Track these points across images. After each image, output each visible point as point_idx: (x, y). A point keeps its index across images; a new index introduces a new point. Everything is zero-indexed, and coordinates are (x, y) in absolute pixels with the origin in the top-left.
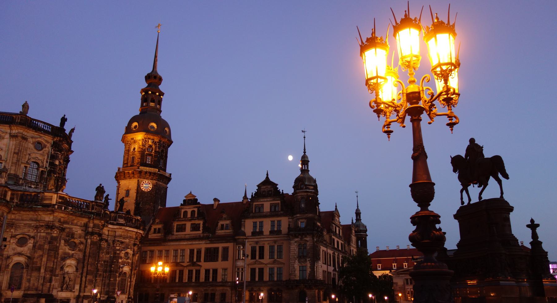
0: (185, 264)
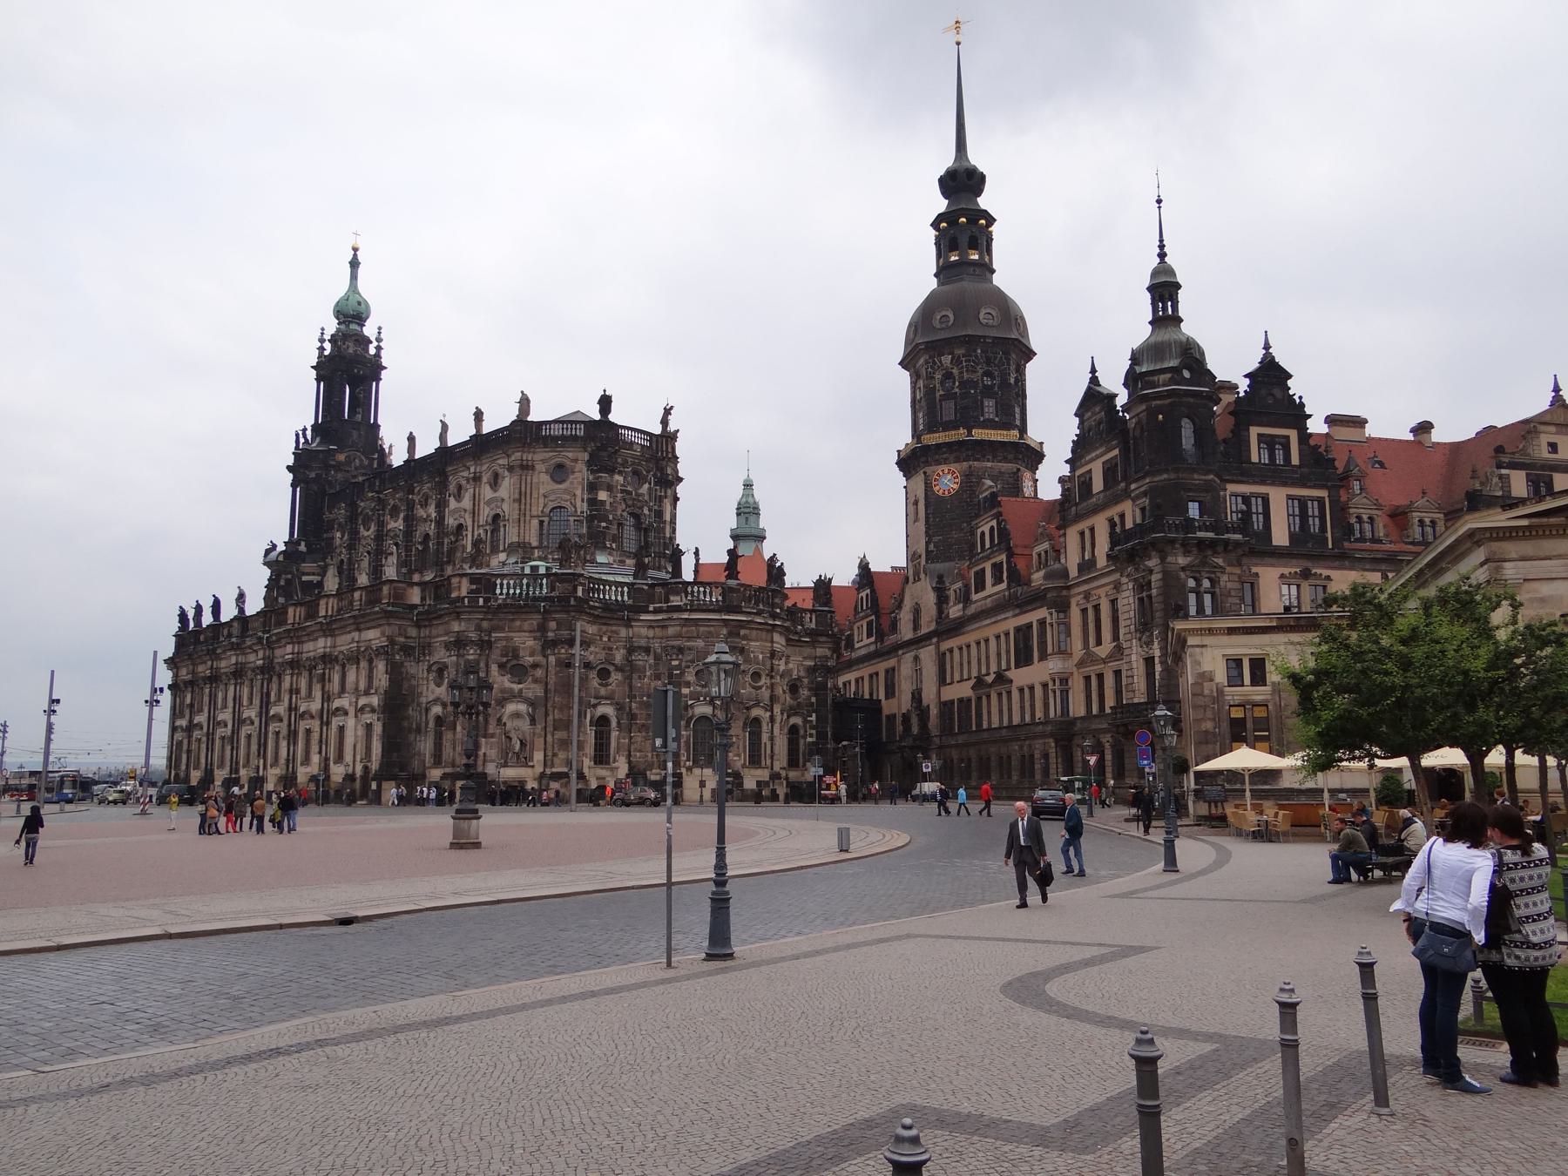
0: (990, 679)
